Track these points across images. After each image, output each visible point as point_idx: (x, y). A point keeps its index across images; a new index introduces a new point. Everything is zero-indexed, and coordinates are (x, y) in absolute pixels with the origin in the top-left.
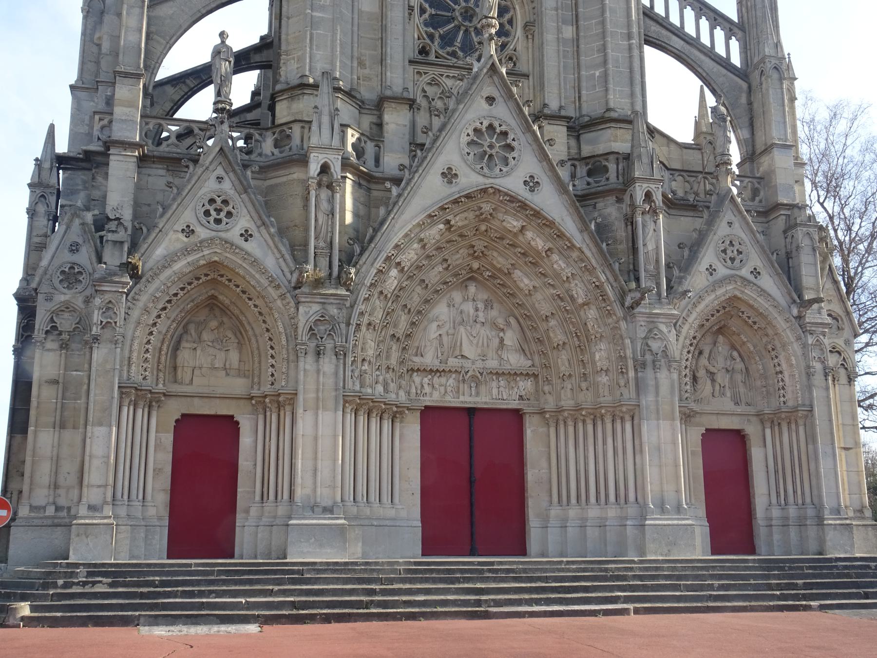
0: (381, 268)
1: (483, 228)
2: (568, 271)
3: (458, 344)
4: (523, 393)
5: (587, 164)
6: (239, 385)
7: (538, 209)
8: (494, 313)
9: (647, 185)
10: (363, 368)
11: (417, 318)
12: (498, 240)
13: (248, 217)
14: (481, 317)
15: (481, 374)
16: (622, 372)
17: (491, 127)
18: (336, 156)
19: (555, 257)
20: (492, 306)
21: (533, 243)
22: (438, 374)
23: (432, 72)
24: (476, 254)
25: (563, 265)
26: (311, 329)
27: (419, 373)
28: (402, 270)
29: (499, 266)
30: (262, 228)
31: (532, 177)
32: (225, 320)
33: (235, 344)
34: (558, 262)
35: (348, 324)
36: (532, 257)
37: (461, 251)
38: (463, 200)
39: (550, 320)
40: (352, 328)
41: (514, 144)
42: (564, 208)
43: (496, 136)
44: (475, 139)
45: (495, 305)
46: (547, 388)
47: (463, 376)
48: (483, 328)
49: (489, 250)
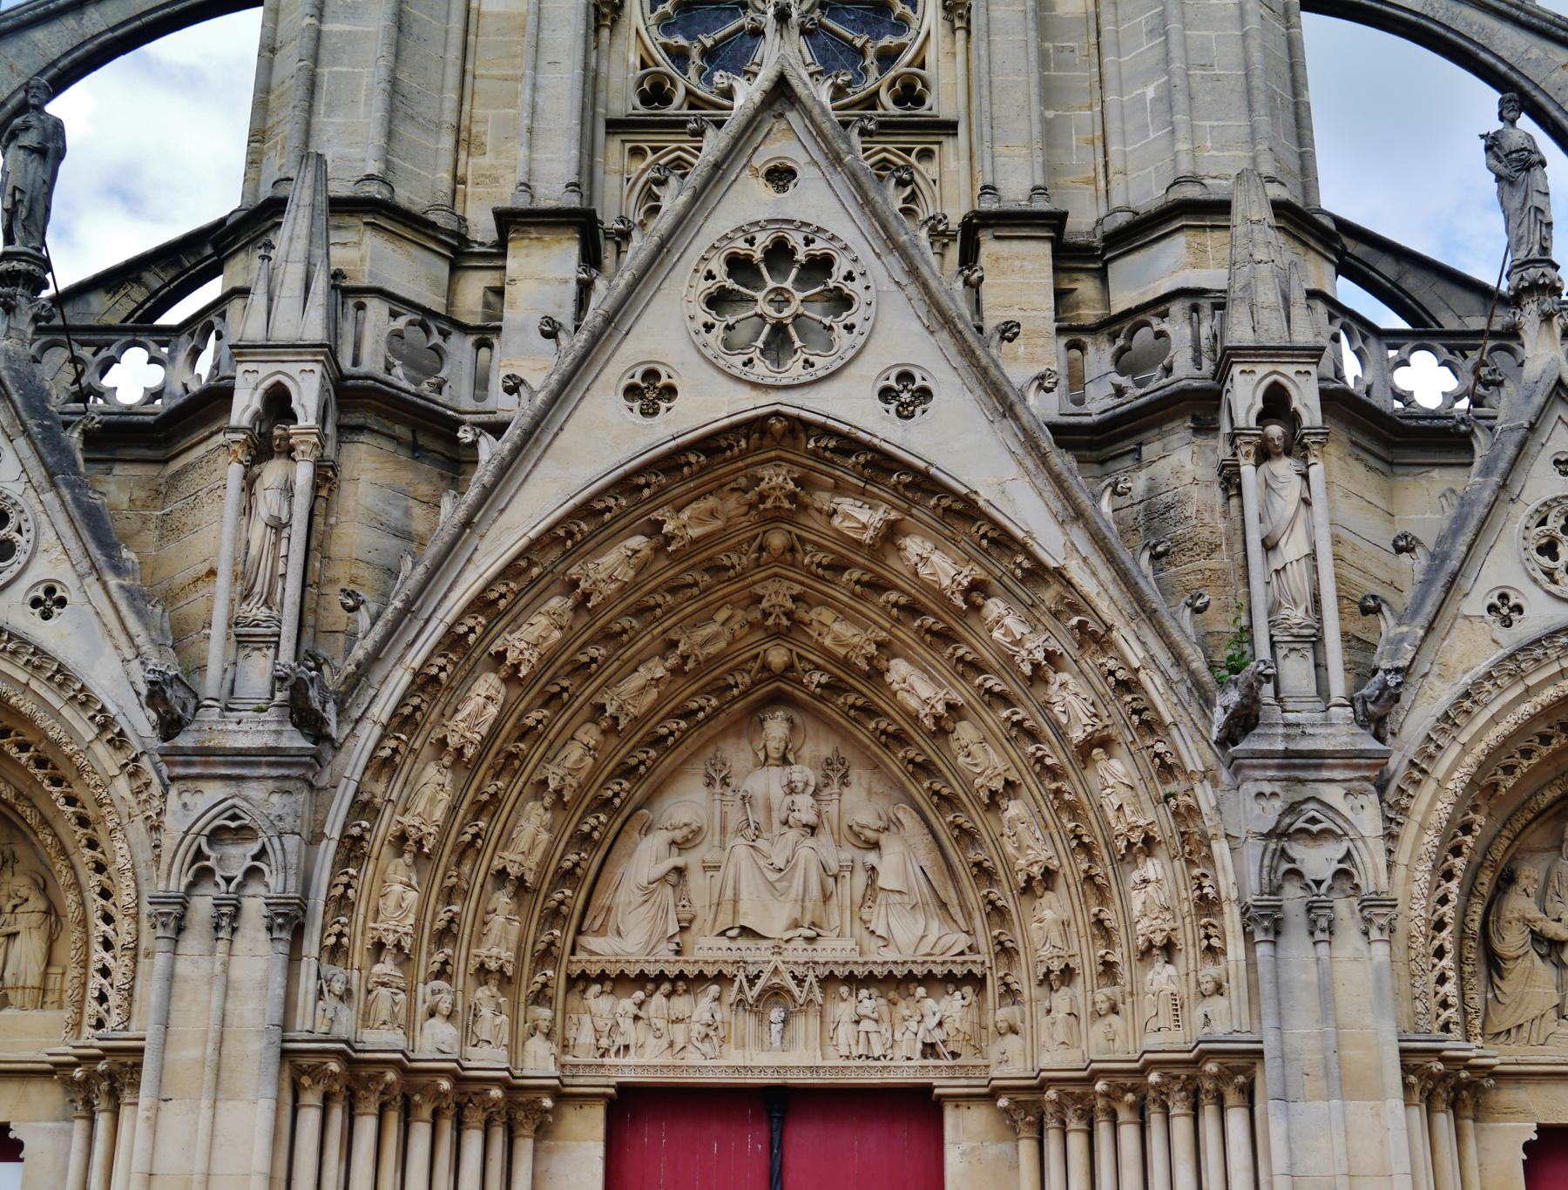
0: (434, 670)
1: (777, 540)
2: (1035, 647)
3: (729, 893)
4: (938, 1036)
5: (1114, 337)
7: (922, 465)
9: (1270, 368)
10: (378, 968)
11: (593, 821)
12: (828, 575)
13: (57, 552)
14: (805, 808)
15: (800, 982)
16: (1210, 948)
17: (780, 253)
18: (309, 366)
19: (994, 607)
20: (845, 776)
21: (924, 571)
22: (666, 987)
23: (674, 145)
24: (770, 622)
25: (1018, 629)
26: (199, 856)
27: (608, 986)
28: (512, 678)
29: (842, 651)
30: (92, 579)
31: (906, 377)
32: (21, 851)
33: (36, 917)
35: (316, 838)
36: (935, 615)
37: (723, 614)
38: (693, 458)
39: (1004, 803)
40: (327, 851)
41: (848, 287)
42: (1007, 455)
43: (794, 272)
44: (730, 284)
45: (854, 776)
46: (1005, 1013)
47: (741, 990)
48: (810, 842)
49: (811, 607)
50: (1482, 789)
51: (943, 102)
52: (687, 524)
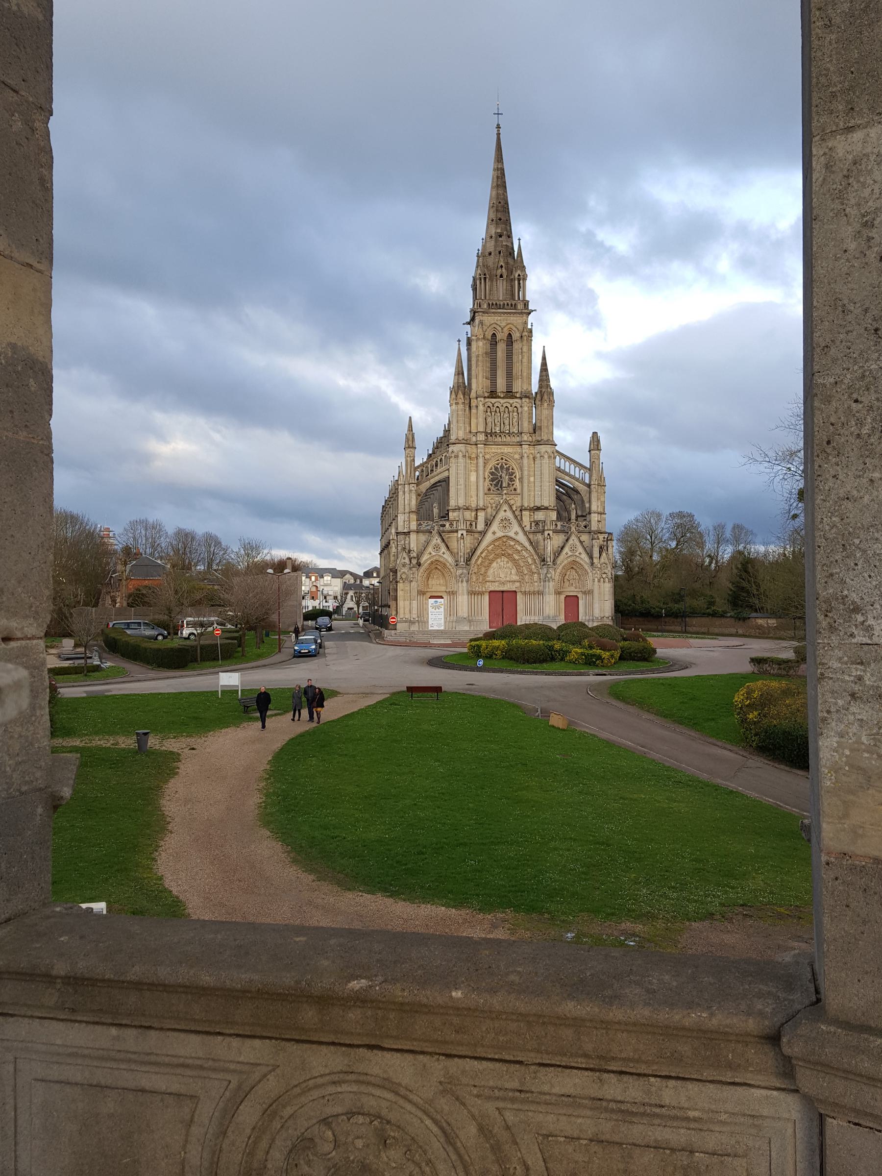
2: (527, 555)
6: (443, 589)
8: (508, 565)
34: (524, 553)
50: (563, 568)
51: (519, 491)
52: (496, 544)
